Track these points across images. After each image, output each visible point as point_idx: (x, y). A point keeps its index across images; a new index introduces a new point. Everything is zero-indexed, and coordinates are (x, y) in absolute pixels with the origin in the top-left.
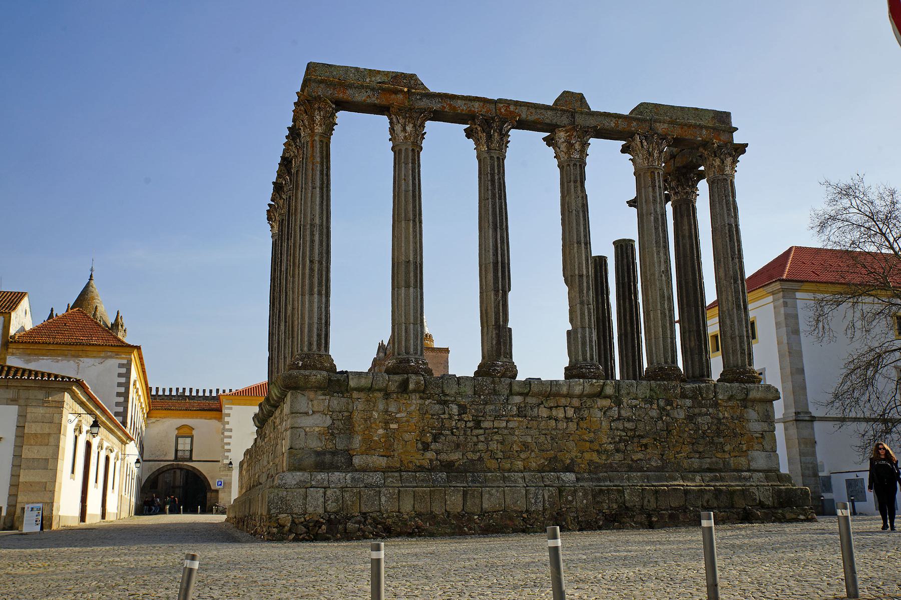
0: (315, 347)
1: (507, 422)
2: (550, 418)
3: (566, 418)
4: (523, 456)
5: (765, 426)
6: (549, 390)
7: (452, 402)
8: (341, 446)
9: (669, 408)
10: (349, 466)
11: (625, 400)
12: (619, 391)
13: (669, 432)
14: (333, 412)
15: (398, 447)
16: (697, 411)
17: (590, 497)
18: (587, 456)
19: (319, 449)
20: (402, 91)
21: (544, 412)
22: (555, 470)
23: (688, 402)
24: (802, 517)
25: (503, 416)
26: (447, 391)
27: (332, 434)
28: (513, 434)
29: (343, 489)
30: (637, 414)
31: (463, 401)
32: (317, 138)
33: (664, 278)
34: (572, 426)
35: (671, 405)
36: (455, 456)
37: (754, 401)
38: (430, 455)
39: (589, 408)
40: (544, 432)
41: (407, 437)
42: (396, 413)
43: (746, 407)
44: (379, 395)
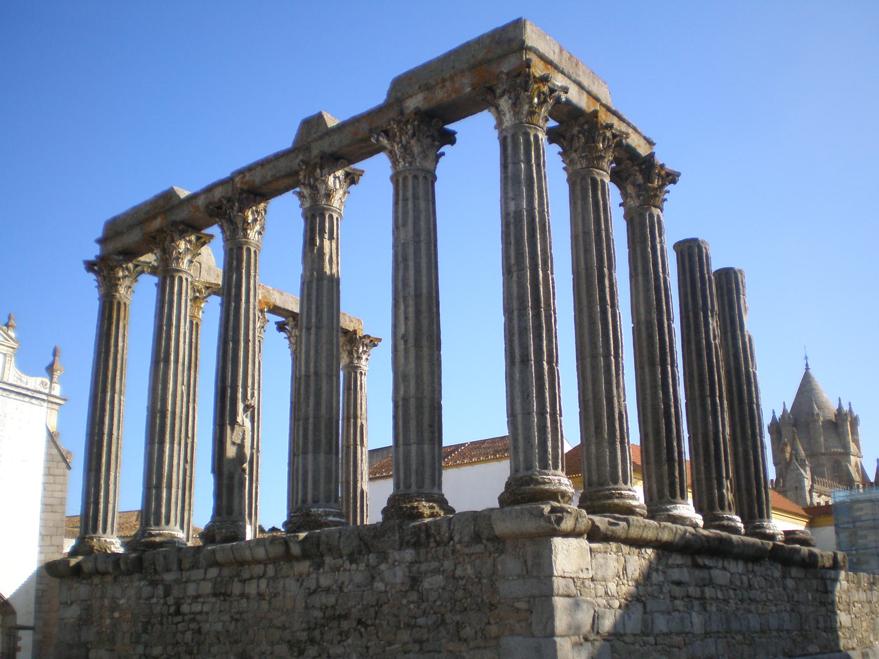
2: (243, 595)
6: (231, 556)
9: (383, 567)
11: (328, 560)
12: (318, 545)
16: (424, 567)
23: (409, 554)
26: (159, 569)
28: (207, 621)
31: (169, 577)
34: (265, 605)
35: (387, 562)
38: (140, 649)
43: (502, 553)
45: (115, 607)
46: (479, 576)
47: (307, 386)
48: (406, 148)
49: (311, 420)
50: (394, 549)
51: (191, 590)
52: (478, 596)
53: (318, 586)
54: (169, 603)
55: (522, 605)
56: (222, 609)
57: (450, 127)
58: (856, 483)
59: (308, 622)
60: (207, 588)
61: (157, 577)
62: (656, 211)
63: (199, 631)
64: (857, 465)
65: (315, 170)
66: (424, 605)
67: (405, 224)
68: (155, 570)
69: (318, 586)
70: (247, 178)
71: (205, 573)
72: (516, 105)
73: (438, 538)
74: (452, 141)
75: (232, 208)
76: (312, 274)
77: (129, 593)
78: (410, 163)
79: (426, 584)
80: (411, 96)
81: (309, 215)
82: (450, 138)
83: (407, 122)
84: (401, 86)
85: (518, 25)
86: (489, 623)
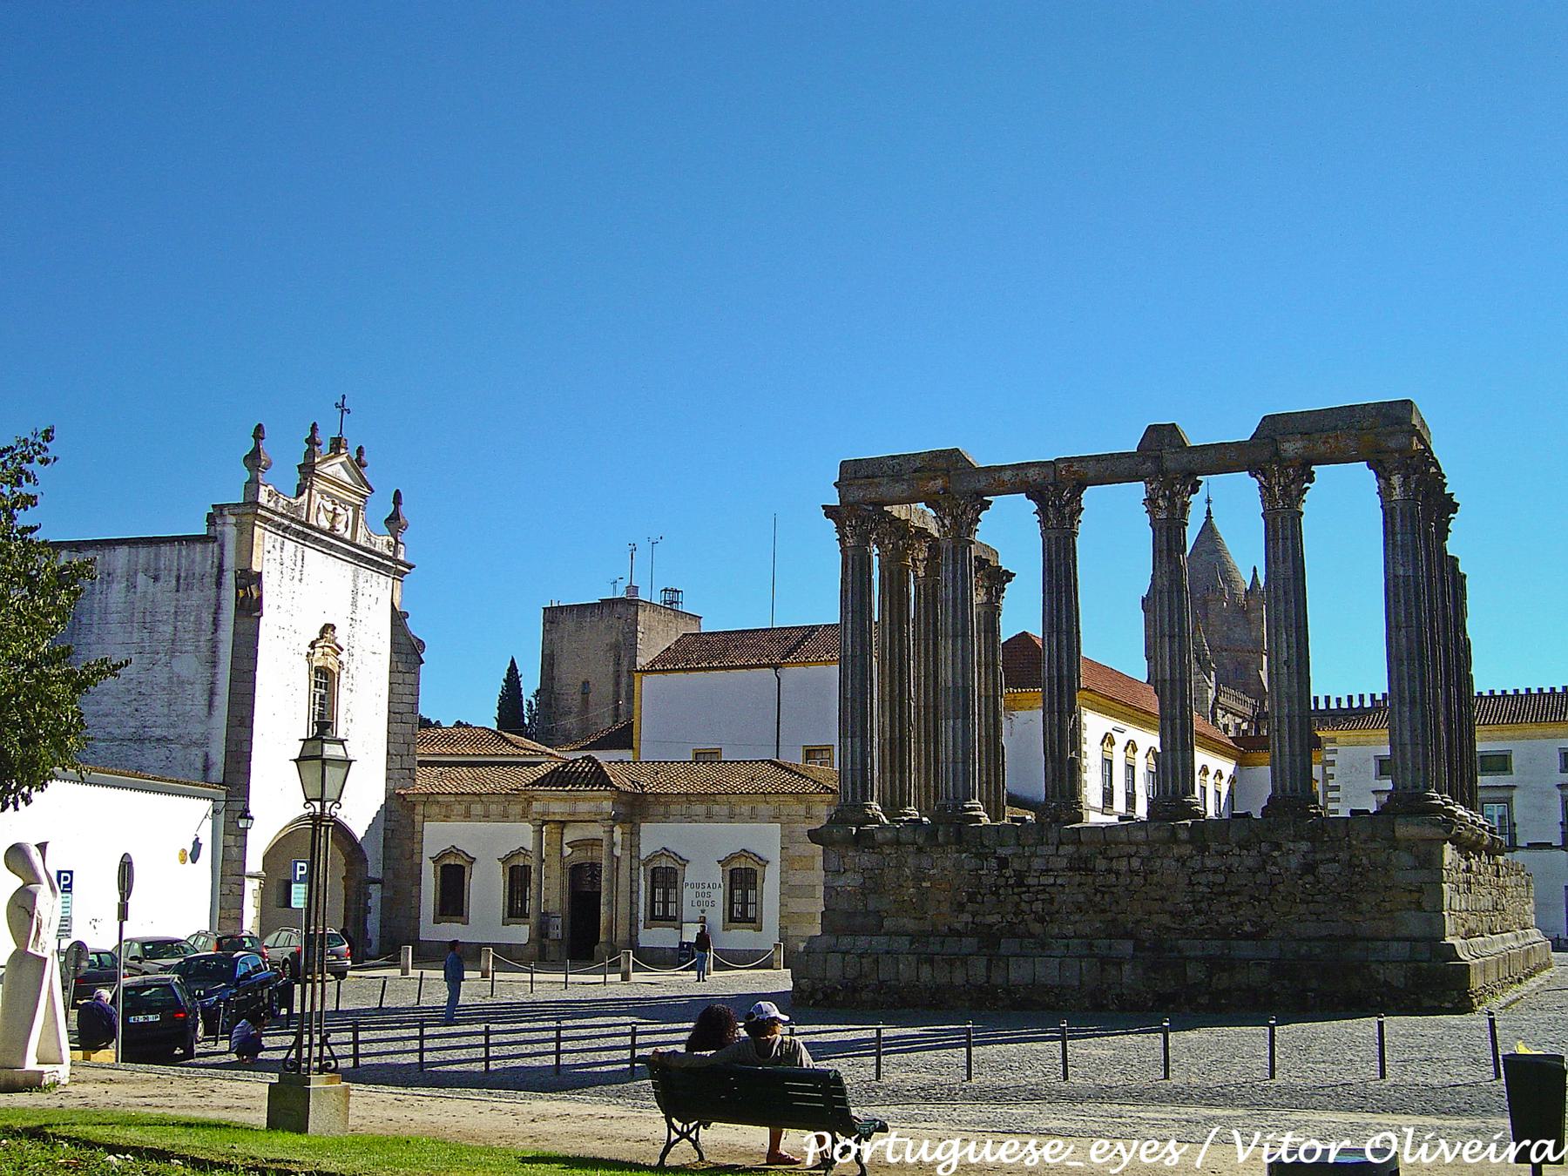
2: (1109, 871)
5: (1423, 875)
8: (871, 907)
9: (1276, 854)
10: (878, 930)
11: (1213, 845)
13: (1273, 886)
16: (1318, 856)
17: (1140, 971)
18: (1156, 919)
21: (1101, 864)
22: (1109, 937)
23: (1304, 846)
24: (1447, 1005)
26: (986, 843)
29: (861, 956)
35: (1278, 846)
38: (966, 917)
48: (1285, 489)
51: (1037, 863)
57: (1313, 468)
60: (1064, 863)
72: (1404, 484)
77: (947, 863)
79: (1321, 869)
81: (1165, 526)
84: (1274, 428)
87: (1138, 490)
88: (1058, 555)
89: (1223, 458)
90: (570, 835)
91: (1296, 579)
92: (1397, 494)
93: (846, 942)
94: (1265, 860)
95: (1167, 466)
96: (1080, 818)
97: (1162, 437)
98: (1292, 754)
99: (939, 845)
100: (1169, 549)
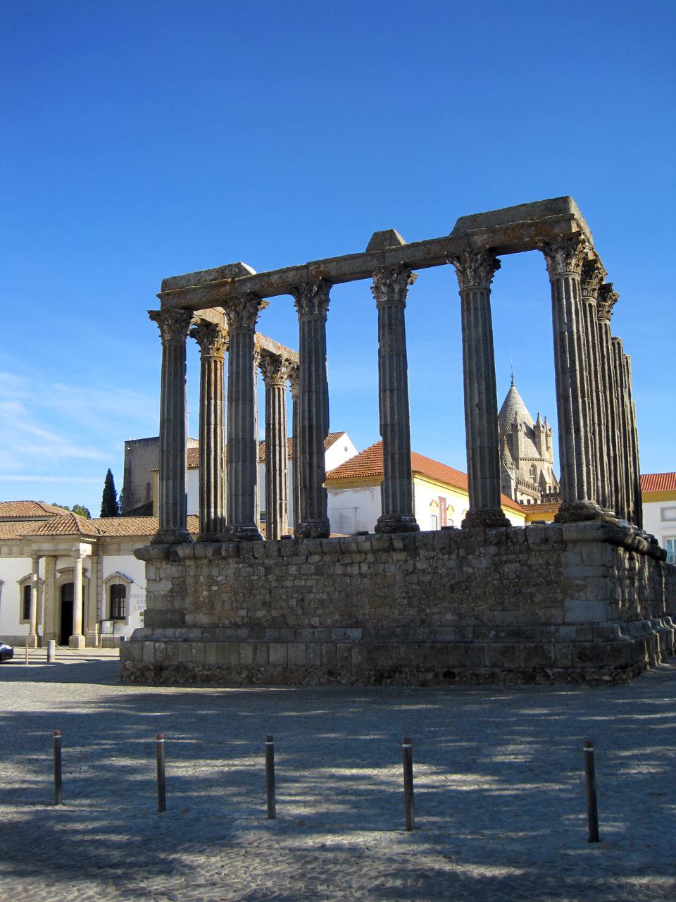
0: (165, 525)
1: (306, 580)
2: (345, 575)
3: (360, 574)
4: (319, 612)
7: (262, 564)
8: (177, 606)
9: (470, 557)
11: (422, 552)
12: (415, 542)
14: (173, 578)
15: (218, 607)
16: (504, 558)
19: (163, 609)
20: (226, 282)
23: (492, 550)
24: (607, 678)
25: (304, 575)
26: (257, 556)
27: (171, 596)
28: (310, 592)
30: (434, 566)
31: (268, 562)
32: (167, 345)
33: (477, 412)
35: (473, 553)
36: (261, 614)
37: (575, 542)
39: (384, 563)
40: (339, 589)
41: (225, 597)
42: (217, 577)
43: (565, 550)
44: (205, 562)
45: (211, 581)
46: (548, 564)
47: (393, 430)
49: (397, 456)
50: (480, 546)
52: (547, 576)
53: (415, 569)
54: (271, 579)
55: (580, 582)
56: (326, 583)
57: (498, 257)
58: (548, 486)
59: (408, 592)
61: (257, 561)
62: (607, 322)
63: (303, 600)
64: (548, 469)
65: (392, 275)
66: (505, 582)
67: (476, 326)
68: (253, 555)
69: (415, 569)
70: (322, 268)
71: (307, 559)
73: (514, 540)
74: (499, 267)
75: (311, 290)
76: (391, 351)
78: (479, 283)
79: (506, 568)
80: (477, 235)
82: (497, 265)
83: (477, 254)
84: (466, 226)
85: (565, 200)
86: (556, 593)
87: (370, 282)
88: (309, 334)
89: (430, 254)
90: (61, 564)
91: (485, 340)
92: (561, 268)
93: (159, 631)
94: (462, 561)
95: (390, 266)
96: (325, 534)
97: (383, 240)
98: (483, 478)
99: (224, 558)
100: (390, 324)
